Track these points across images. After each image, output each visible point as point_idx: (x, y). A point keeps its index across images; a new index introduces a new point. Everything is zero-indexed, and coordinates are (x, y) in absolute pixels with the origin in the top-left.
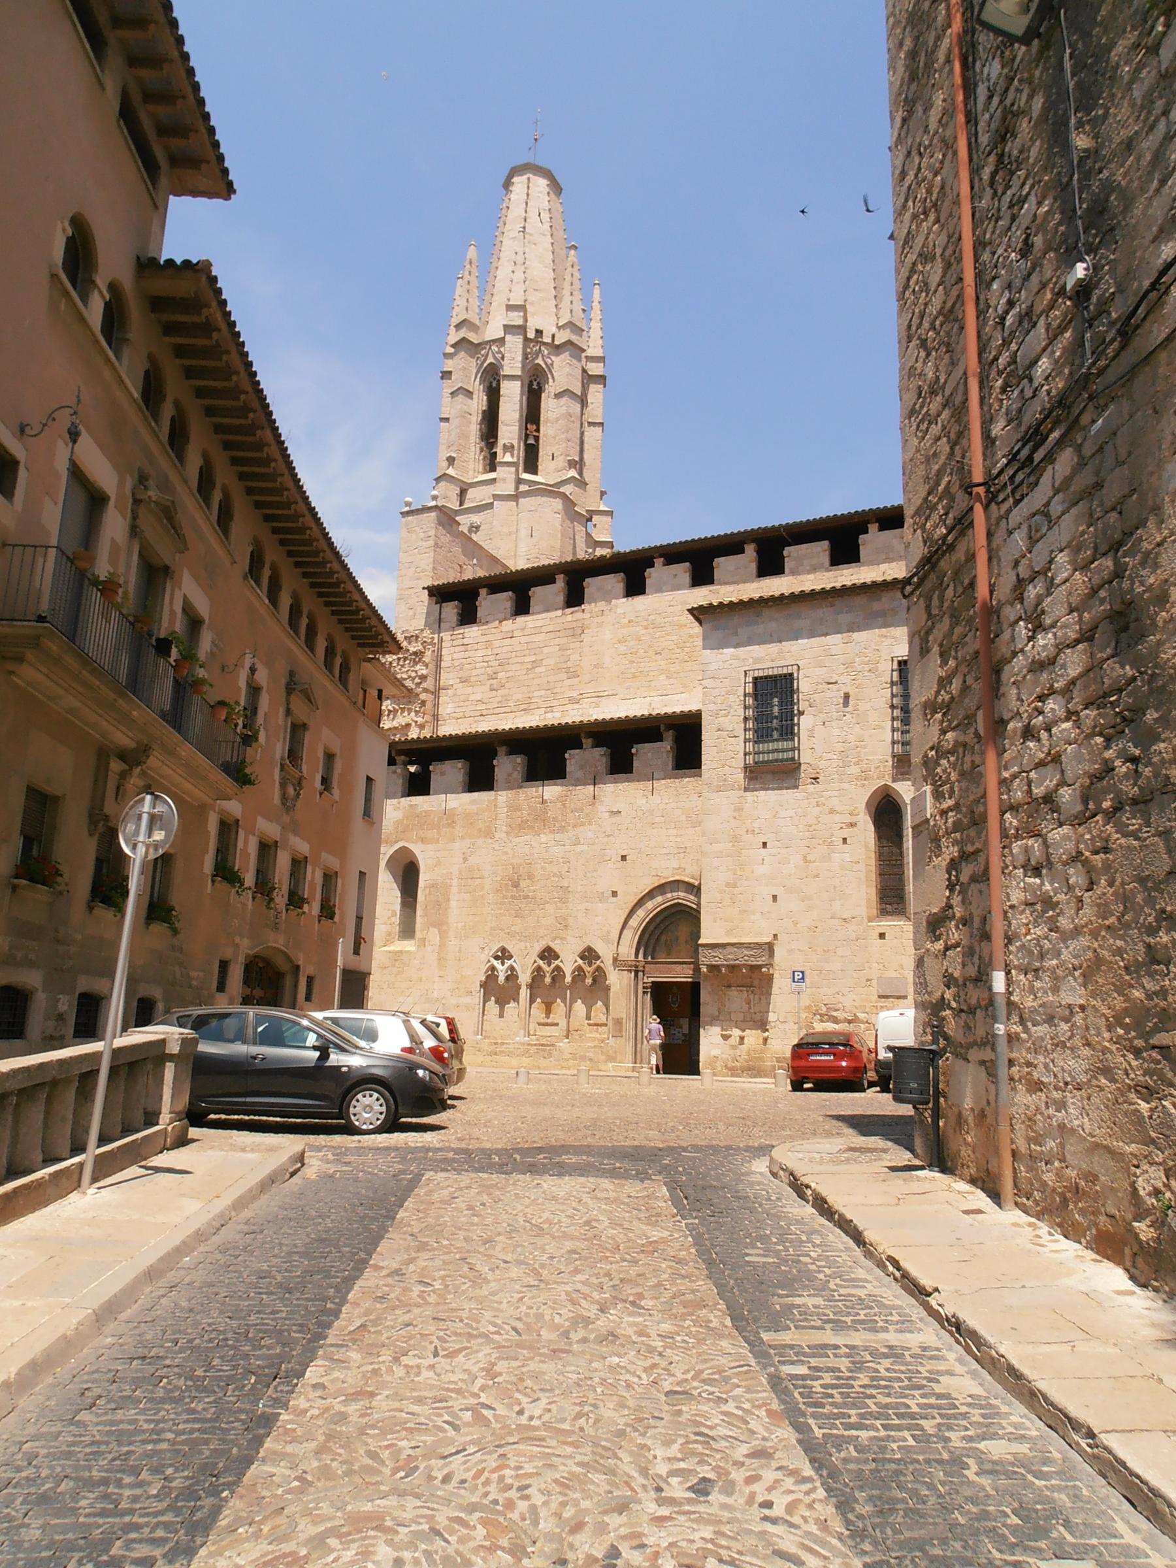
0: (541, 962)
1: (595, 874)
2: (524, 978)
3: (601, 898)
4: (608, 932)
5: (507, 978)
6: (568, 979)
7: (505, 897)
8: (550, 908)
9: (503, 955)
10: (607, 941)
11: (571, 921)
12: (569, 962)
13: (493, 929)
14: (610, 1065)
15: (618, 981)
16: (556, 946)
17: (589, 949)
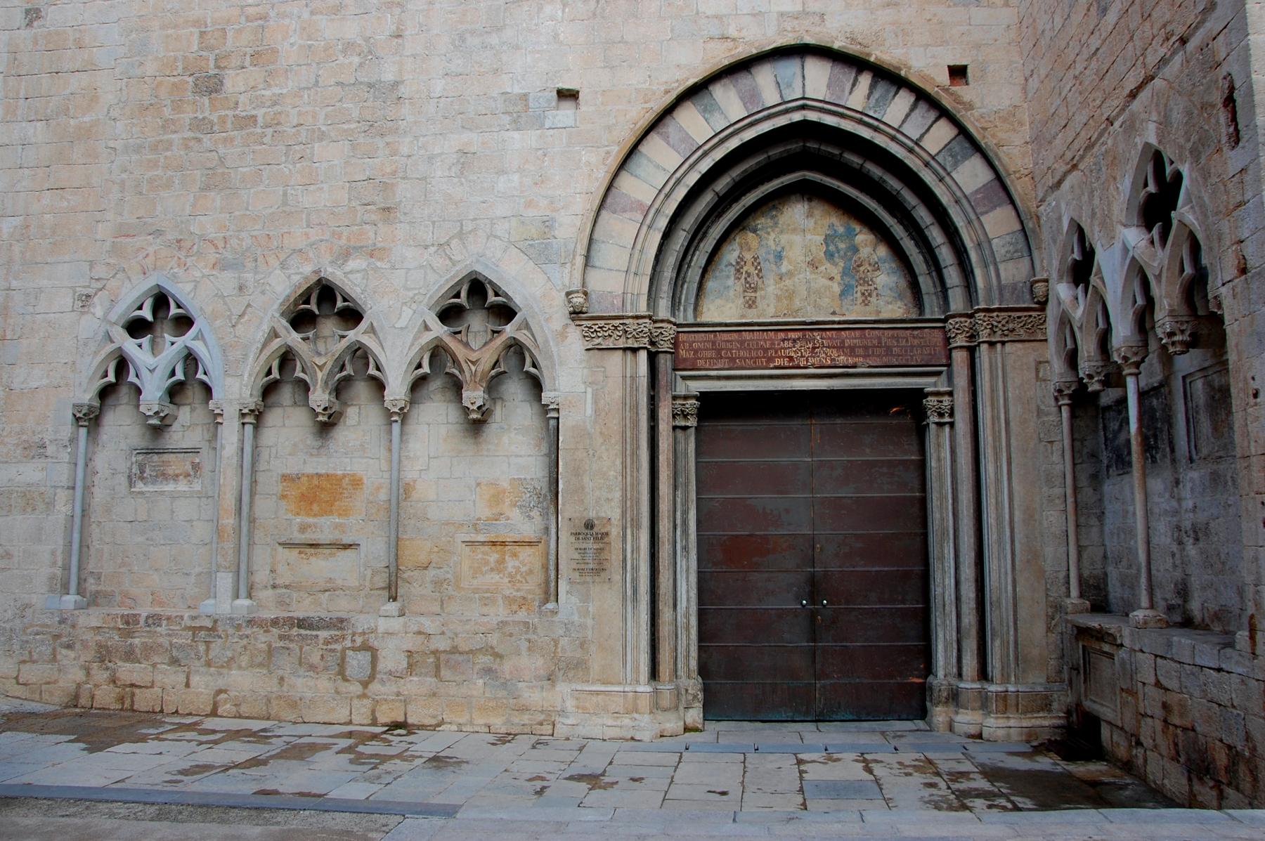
0: (294, 338)
1: (494, 40)
2: (235, 387)
3: (520, 111)
4: (548, 224)
5: (175, 392)
6: (397, 388)
7: (166, 126)
8: (330, 155)
9: (161, 315)
10: (540, 249)
11: (404, 192)
12: (399, 332)
13: (124, 232)
14: (563, 688)
15: (588, 385)
16: (352, 279)
17: (477, 287)
